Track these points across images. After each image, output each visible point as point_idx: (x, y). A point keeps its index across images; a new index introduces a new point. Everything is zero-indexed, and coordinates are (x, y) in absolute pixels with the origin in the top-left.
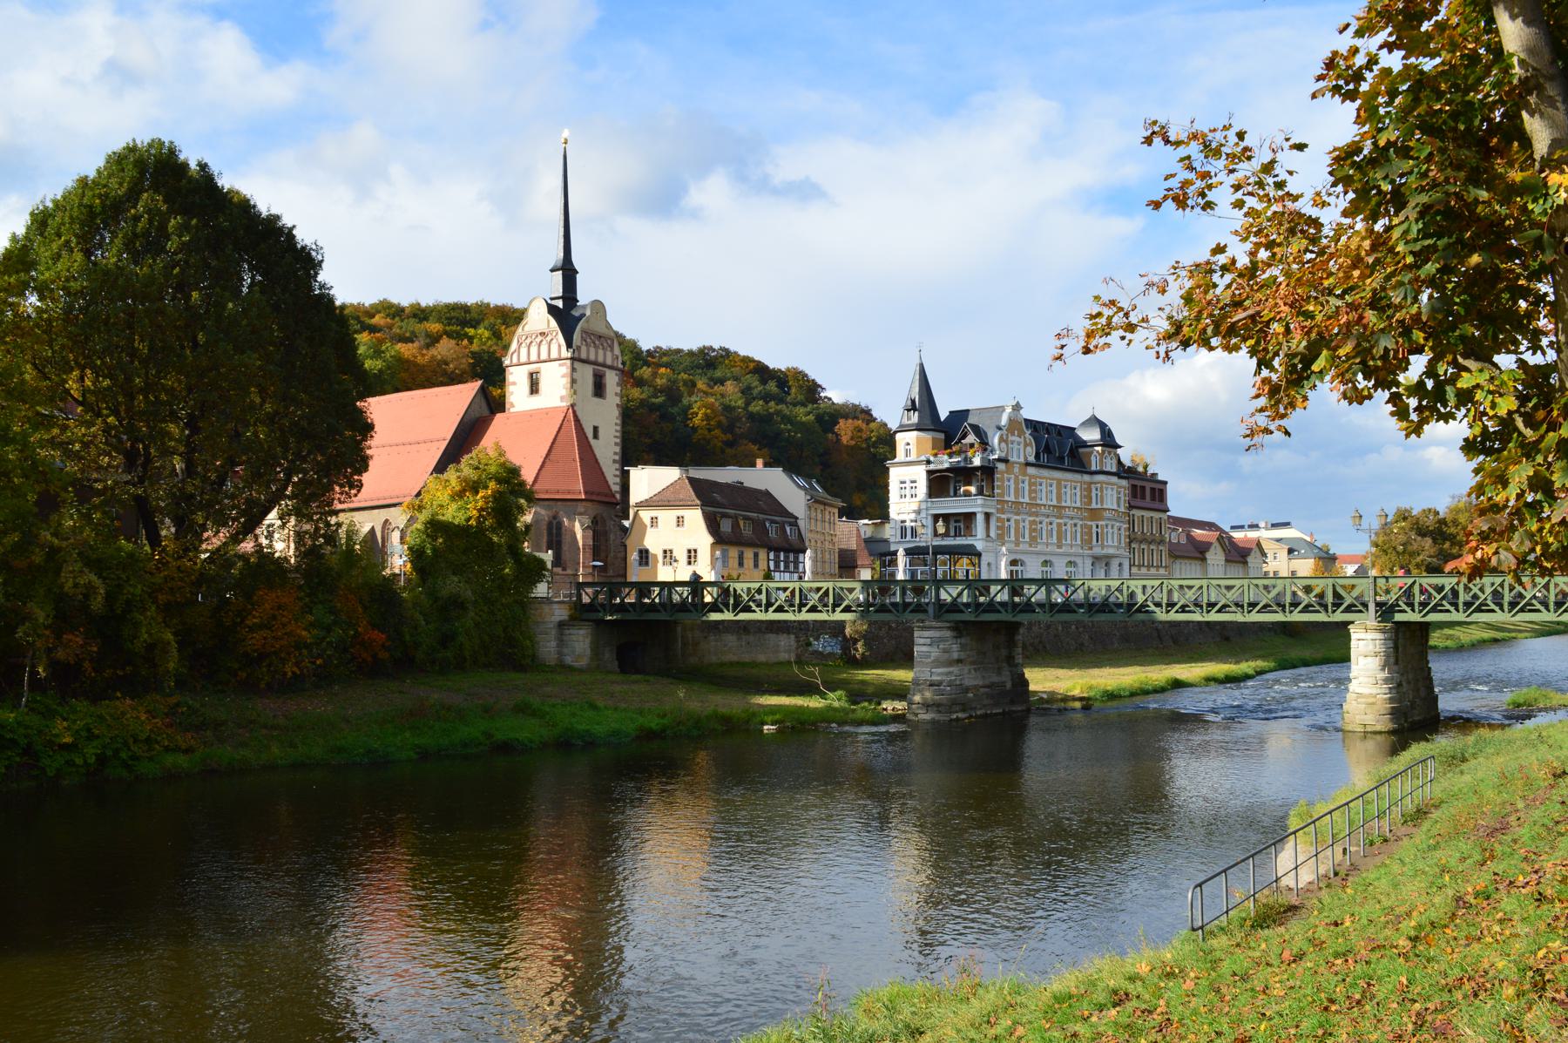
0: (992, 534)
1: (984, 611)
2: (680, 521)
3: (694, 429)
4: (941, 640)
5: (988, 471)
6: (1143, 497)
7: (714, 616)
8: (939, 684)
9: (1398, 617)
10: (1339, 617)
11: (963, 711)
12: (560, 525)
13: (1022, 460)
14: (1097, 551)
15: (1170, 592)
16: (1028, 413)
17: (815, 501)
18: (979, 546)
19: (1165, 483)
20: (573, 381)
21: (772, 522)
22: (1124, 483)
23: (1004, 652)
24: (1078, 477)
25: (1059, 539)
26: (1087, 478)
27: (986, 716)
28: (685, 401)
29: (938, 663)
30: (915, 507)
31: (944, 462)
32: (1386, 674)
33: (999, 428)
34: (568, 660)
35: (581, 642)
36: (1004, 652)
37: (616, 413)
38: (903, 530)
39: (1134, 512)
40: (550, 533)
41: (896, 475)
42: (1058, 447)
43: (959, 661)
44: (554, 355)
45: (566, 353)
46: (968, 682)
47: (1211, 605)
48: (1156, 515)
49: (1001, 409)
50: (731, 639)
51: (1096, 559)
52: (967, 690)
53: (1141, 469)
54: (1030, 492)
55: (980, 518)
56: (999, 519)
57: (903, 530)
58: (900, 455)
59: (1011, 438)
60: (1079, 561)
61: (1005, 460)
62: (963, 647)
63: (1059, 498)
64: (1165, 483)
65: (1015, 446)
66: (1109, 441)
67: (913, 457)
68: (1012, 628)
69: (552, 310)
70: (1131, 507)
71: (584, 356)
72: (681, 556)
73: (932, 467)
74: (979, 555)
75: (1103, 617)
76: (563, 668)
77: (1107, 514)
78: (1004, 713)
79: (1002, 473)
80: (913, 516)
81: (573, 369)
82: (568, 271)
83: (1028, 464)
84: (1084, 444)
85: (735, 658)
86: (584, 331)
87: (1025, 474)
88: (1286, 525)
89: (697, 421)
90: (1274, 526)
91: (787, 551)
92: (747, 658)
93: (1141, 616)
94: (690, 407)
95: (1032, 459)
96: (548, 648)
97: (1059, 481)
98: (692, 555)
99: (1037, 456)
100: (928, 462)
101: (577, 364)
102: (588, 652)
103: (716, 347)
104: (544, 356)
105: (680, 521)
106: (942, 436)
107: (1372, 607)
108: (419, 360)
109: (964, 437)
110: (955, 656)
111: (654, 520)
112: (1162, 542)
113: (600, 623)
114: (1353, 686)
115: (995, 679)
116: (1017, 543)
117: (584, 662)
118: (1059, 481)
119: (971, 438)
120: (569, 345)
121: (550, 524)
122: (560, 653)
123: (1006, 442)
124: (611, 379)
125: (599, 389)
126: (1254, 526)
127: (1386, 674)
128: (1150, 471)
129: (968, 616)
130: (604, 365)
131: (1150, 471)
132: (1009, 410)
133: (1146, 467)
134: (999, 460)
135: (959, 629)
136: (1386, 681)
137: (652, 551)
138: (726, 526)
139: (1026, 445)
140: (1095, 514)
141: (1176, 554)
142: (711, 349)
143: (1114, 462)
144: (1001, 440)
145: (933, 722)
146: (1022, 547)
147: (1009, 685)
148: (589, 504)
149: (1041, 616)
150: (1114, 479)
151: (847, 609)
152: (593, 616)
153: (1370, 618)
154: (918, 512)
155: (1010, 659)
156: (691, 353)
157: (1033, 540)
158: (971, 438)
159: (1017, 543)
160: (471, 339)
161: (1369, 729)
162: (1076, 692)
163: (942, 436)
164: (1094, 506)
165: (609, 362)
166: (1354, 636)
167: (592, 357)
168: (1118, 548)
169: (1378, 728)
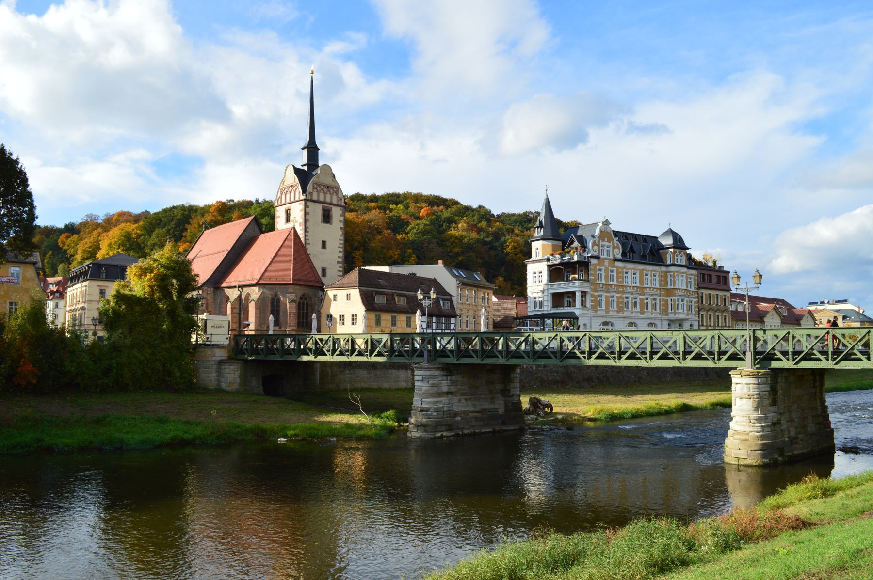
0: (588, 305)
1: (513, 357)
2: (348, 297)
3: (507, 254)
4: (430, 377)
5: (584, 265)
6: (710, 281)
7: (305, 358)
8: (427, 410)
9: (775, 364)
10: (724, 363)
11: (450, 430)
12: (279, 299)
13: (611, 257)
14: (672, 316)
15: (562, 341)
16: (615, 227)
17: (464, 284)
18: (577, 312)
19: (729, 272)
20: (306, 213)
21: (399, 295)
22: (694, 272)
23: (498, 387)
24: (657, 268)
25: (641, 308)
26: (663, 269)
27: (474, 434)
28: (503, 239)
29: (427, 394)
30: (541, 288)
31: (557, 259)
32: (759, 414)
33: (593, 236)
34: (223, 386)
35: (232, 375)
36: (498, 387)
37: (340, 232)
38: (535, 303)
40: (273, 305)
41: (531, 268)
42: (641, 249)
43: (448, 393)
44: (297, 198)
45: (303, 197)
46: (455, 409)
47: (721, 353)
48: (721, 293)
49: (596, 224)
50: (363, 373)
51: (671, 322)
52: (456, 414)
53: (710, 264)
54: (618, 278)
55: (578, 295)
56: (592, 296)
57: (535, 303)
58: (534, 257)
59: (602, 243)
60: (658, 323)
61: (598, 258)
62: (453, 383)
63: (641, 282)
64: (729, 272)
65: (605, 248)
66: (679, 244)
67: (540, 257)
68: (507, 371)
69: (297, 171)
70: (699, 288)
71: (315, 197)
72: (348, 320)
73: (550, 263)
74: (577, 318)
75: (542, 362)
76: (219, 391)
77: (679, 292)
78: (494, 432)
79: (595, 265)
80: (540, 294)
81: (306, 206)
82: (312, 149)
83: (615, 260)
84: (662, 247)
85: (365, 385)
86: (314, 183)
87: (613, 266)
88: (845, 301)
89: (508, 250)
90: (838, 302)
91: (438, 316)
92: (375, 385)
93: (573, 362)
94: (505, 242)
95: (619, 256)
96: (209, 377)
97: (641, 271)
98: (354, 318)
99: (624, 254)
100: (548, 260)
101: (309, 203)
102: (238, 380)
103: (533, 211)
104: (292, 200)
105: (348, 297)
106: (560, 243)
107: (749, 356)
108: (357, 221)
109: (572, 242)
110: (445, 389)
111: (335, 296)
112: (726, 310)
113: (247, 362)
114: (732, 425)
115: (487, 406)
116: (607, 311)
117: (235, 387)
118: (641, 271)
119: (576, 244)
120: (304, 191)
121: (273, 299)
122: (219, 381)
123: (598, 245)
124: (336, 213)
125: (327, 218)
126: (822, 303)
127: (759, 414)
128: (718, 265)
129: (452, 360)
130: (331, 204)
131: (718, 265)
132: (601, 225)
133: (715, 262)
134: (592, 257)
135: (448, 370)
136: (759, 420)
137: (334, 316)
138: (380, 300)
139: (614, 247)
140: (670, 292)
141: (738, 317)
142: (530, 212)
143: (684, 258)
144: (594, 244)
145: (421, 439)
146: (611, 313)
147: (502, 411)
148: (298, 287)
149: (525, 362)
150: (685, 270)
151: (380, 354)
152: (241, 357)
153: (747, 365)
154: (543, 292)
155: (505, 392)
156: (519, 215)
157: (620, 309)
158: (576, 244)
159: (607, 311)
160: (391, 210)
161: (742, 462)
162: (589, 415)
163: (560, 243)
164: (669, 287)
165: (335, 201)
166: (734, 380)
167: (322, 199)
168: (688, 314)
169: (749, 462)
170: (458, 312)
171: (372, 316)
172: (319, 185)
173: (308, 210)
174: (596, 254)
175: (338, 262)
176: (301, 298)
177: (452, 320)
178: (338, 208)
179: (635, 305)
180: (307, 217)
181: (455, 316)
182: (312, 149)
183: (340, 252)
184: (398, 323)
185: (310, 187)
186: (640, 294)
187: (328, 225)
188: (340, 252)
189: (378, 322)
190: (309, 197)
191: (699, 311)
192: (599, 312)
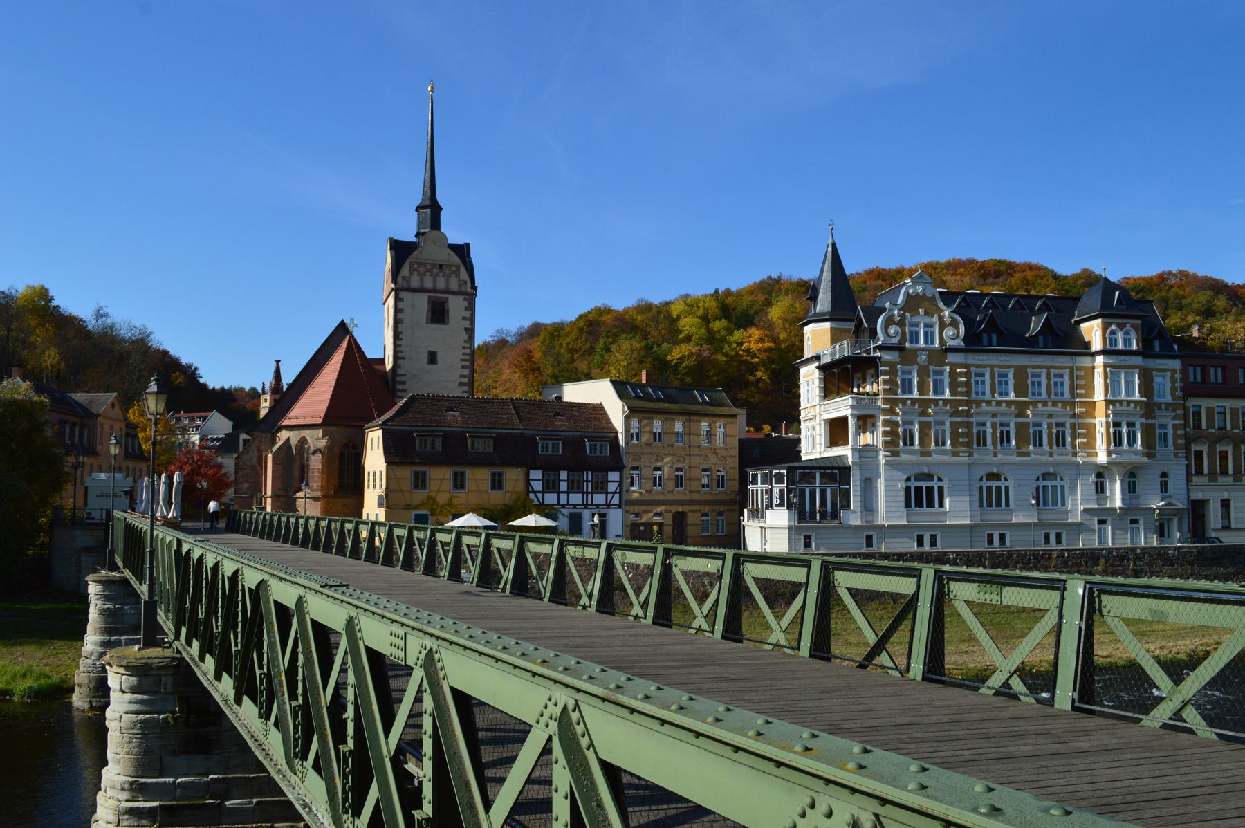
20: (397, 310)
39: (1192, 403)
58: (806, 356)
61: (899, 348)
71: (415, 282)
82: (431, 210)
97: (1020, 372)
101: (402, 294)
103: (1175, 270)
134: (881, 348)
142: (1170, 273)
148: (334, 429)
150: (1138, 360)
165: (454, 285)
167: (428, 283)
171: (406, 473)
172: (420, 264)
174: (895, 341)
175: (461, 384)
176: (346, 446)
177: (613, 476)
178: (461, 298)
179: (1005, 437)
180: (400, 316)
181: (620, 468)
182: (431, 210)
183: (463, 367)
184: (469, 484)
185: (405, 271)
186: (1017, 416)
187: (442, 326)
188: (463, 367)
189: (420, 482)
190: (400, 285)
191: (1187, 448)
192: (903, 456)
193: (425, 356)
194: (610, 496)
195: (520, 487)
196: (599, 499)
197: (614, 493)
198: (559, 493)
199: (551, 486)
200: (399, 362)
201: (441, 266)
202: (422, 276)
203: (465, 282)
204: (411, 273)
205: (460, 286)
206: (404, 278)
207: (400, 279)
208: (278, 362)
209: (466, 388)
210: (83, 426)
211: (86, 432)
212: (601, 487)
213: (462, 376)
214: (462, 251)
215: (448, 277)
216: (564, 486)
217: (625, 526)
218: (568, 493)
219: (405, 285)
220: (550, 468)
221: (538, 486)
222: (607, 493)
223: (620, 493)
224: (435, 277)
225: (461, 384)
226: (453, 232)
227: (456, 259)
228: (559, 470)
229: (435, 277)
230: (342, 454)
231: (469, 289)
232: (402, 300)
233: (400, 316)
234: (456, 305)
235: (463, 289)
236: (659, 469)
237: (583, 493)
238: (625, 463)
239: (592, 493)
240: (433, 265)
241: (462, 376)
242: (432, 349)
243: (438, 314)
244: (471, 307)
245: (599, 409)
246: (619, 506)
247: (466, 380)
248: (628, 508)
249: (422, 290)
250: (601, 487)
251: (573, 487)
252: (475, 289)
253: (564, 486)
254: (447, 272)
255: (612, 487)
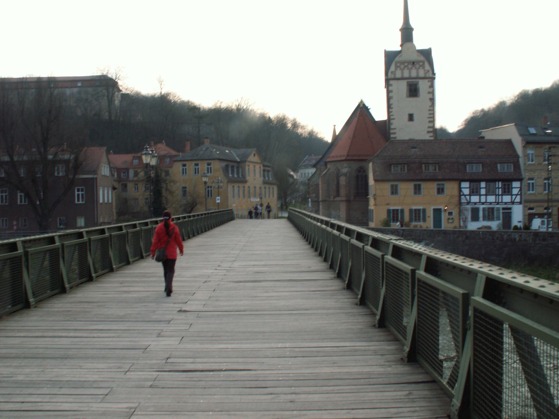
71: (398, 75)
86: (396, 63)
101: (391, 82)
165: (422, 73)
167: (406, 74)
170: (525, 175)
173: (390, 88)
175: (428, 132)
176: (359, 171)
177: (516, 184)
178: (426, 81)
180: (391, 95)
181: (520, 180)
185: (393, 68)
193: (406, 117)
194: (514, 197)
195: (456, 192)
196: (507, 198)
197: (517, 195)
198: (480, 195)
199: (474, 191)
200: (392, 121)
201: (413, 63)
202: (402, 70)
203: (428, 71)
204: (396, 69)
205: (425, 74)
206: (392, 72)
207: (389, 74)
208: (335, 126)
209: (432, 134)
210: (238, 168)
211: (240, 171)
212: (507, 191)
213: (429, 127)
214: (427, 54)
215: (418, 70)
216: (483, 191)
217: (524, 215)
218: (486, 195)
219: (393, 77)
220: (474, 181)
221: (466, 191)
222: (512, 195)
223: (521, 194)
224: (410, 70)
225: (428, 132)
226: (420, 42)
227: (422, 58)
228: (480, 181)
229: (410, 70)
230: (357, 177)
231: (431, 75)
232: (391, 85)
233: (391, 95)
234: (423, 85)
235: (427, 76)
236: (532, 179)
237: (496, 195)
238: (523, 176)
239: (502, 195)
240: (409, 62)
241: (429, 127)
242: (411, 112)
243: (413, 91)
244: (432, 86)
245: (509, 143)
246: (520, 203)
247: (431, 130)
248: (526, 204)
249: (402, 79)
250: (507, 191)
251: (489, 192)
252: (434, 74)
253: (483, 191)
254: (417, 66)
255: (515, 191)
